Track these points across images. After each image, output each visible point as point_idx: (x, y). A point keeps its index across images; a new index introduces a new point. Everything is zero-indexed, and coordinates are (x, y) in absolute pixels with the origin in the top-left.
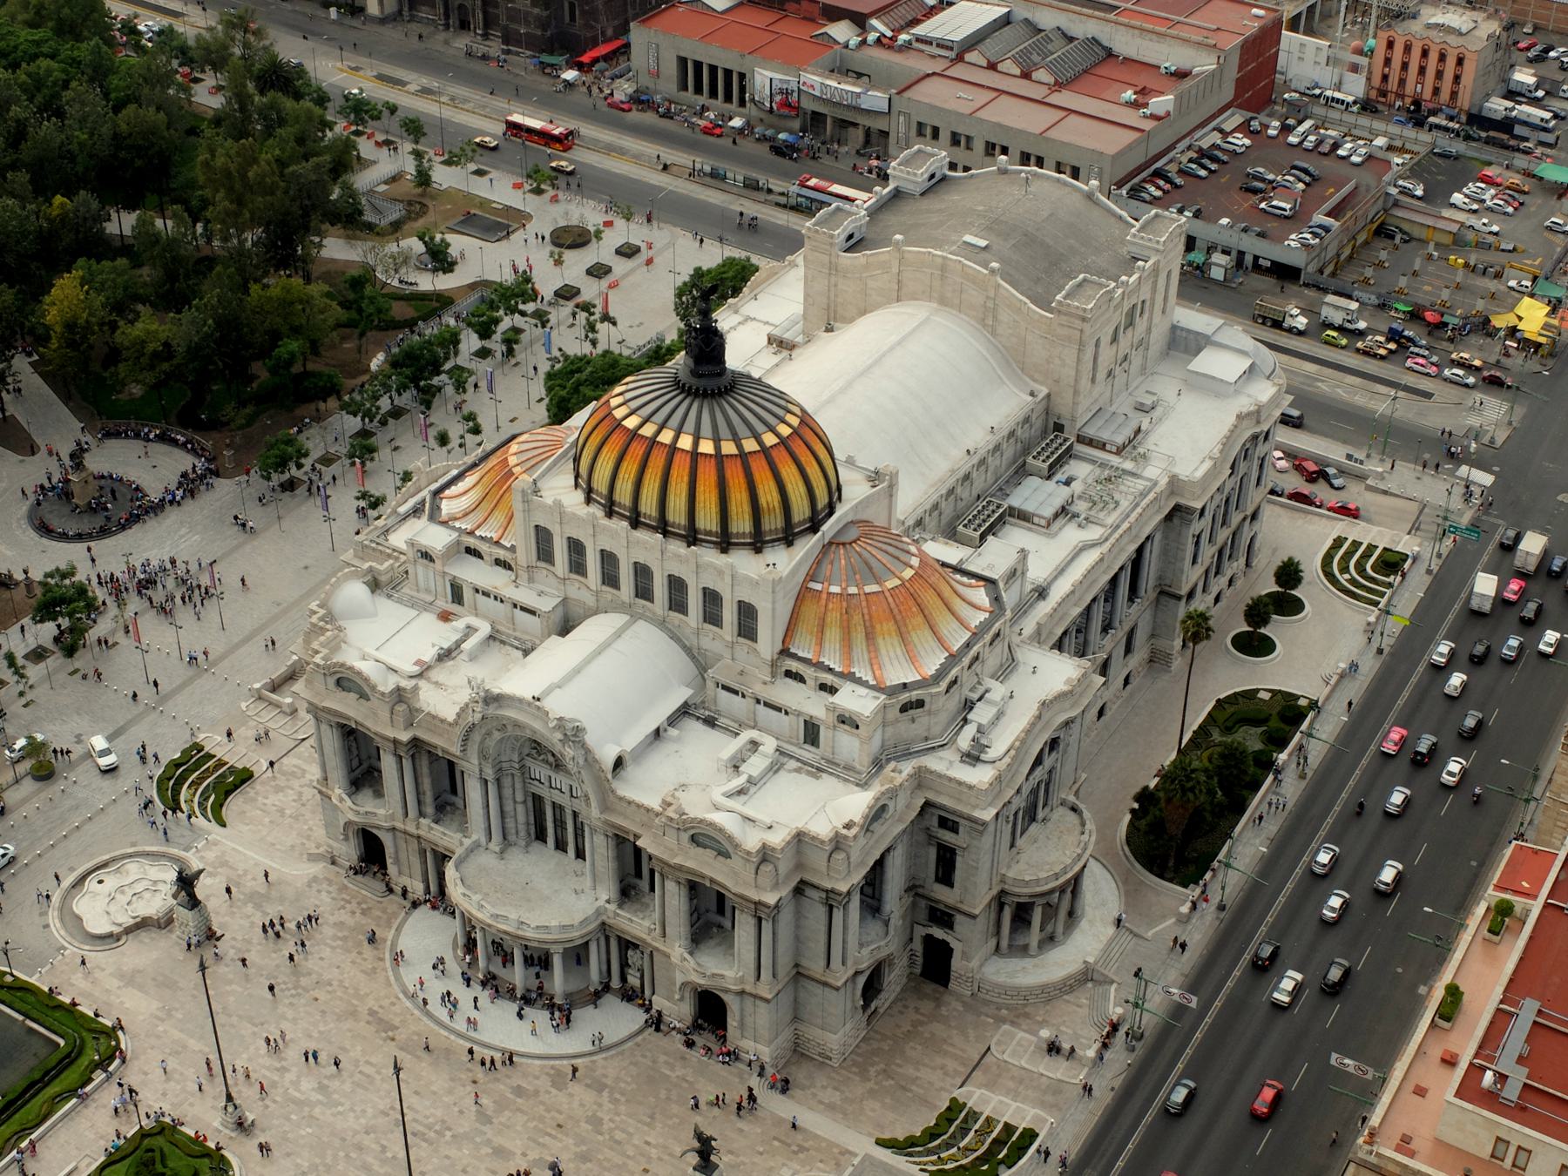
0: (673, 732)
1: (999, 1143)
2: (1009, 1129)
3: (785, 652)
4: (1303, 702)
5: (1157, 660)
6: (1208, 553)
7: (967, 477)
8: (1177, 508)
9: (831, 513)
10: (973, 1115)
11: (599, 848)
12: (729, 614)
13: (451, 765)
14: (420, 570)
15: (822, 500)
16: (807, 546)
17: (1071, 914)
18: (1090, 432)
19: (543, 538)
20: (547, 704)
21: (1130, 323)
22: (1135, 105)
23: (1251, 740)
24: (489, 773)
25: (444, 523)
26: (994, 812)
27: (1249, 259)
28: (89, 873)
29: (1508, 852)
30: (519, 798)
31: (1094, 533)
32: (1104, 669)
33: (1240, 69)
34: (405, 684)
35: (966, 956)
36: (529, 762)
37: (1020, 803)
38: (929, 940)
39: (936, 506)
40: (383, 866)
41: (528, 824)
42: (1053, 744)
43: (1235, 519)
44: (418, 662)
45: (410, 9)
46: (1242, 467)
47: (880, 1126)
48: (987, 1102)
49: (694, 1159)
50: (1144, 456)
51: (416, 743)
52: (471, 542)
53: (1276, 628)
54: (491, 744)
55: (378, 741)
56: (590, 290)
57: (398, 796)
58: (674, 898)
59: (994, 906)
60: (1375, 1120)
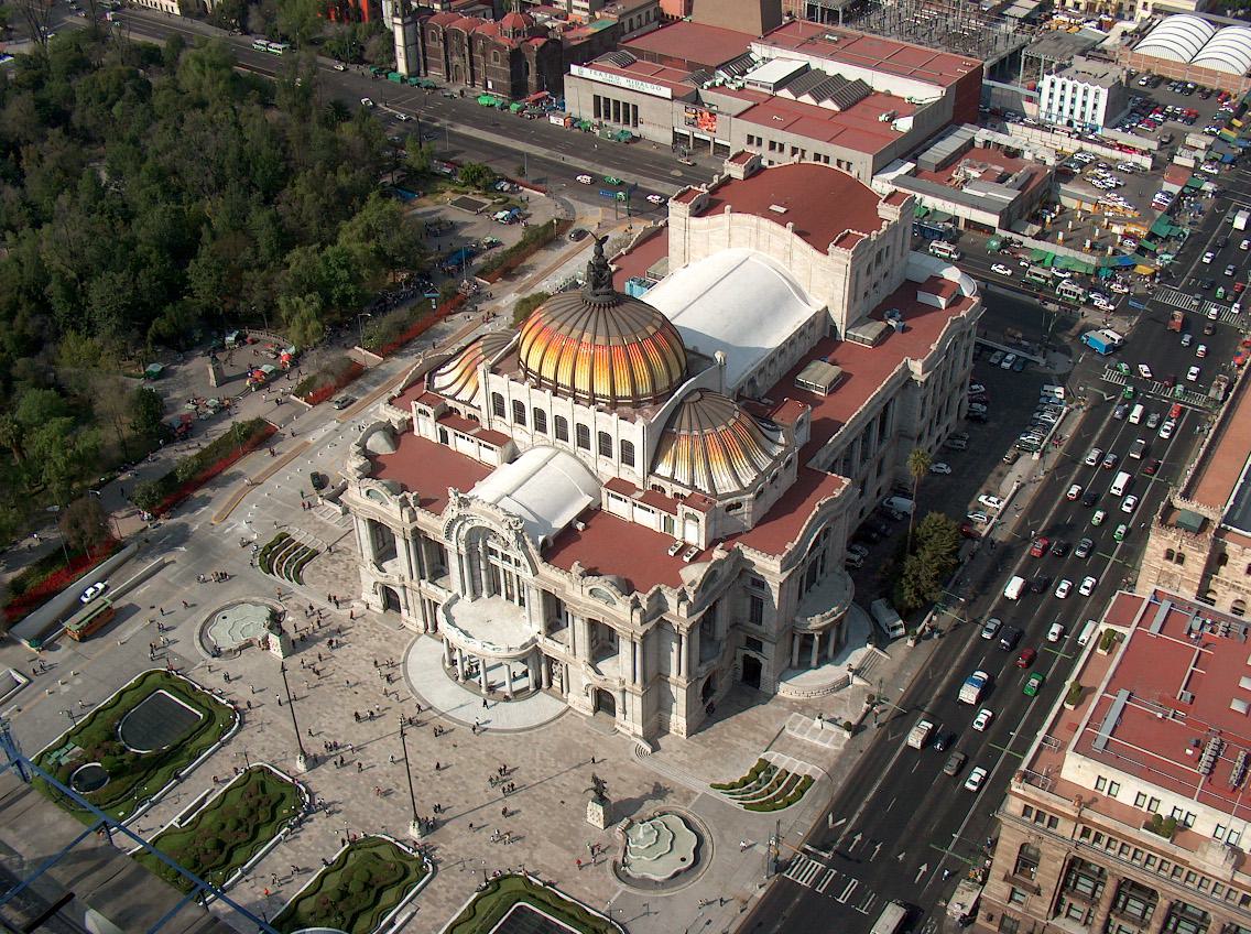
0: (580, 526)
1: (788, 789)
2: (797, 777)
7: (773, 361)
12: (616, 449)
17: (838, 642)
19: (498, 400)
21: (879, 259)
24: (463, 549)
26: (786, 574)
28: (218, 612)
29: (1114, 599)
41: (488, 583)
42: (826, 532)
45: (426, 69)
48: (783, 760)
49: (592, 794)
51: (416, 531)
54: (463, 533)
55: (394, 530)
57: (407, 566)
58: (579, 632)
59: (789, 636)
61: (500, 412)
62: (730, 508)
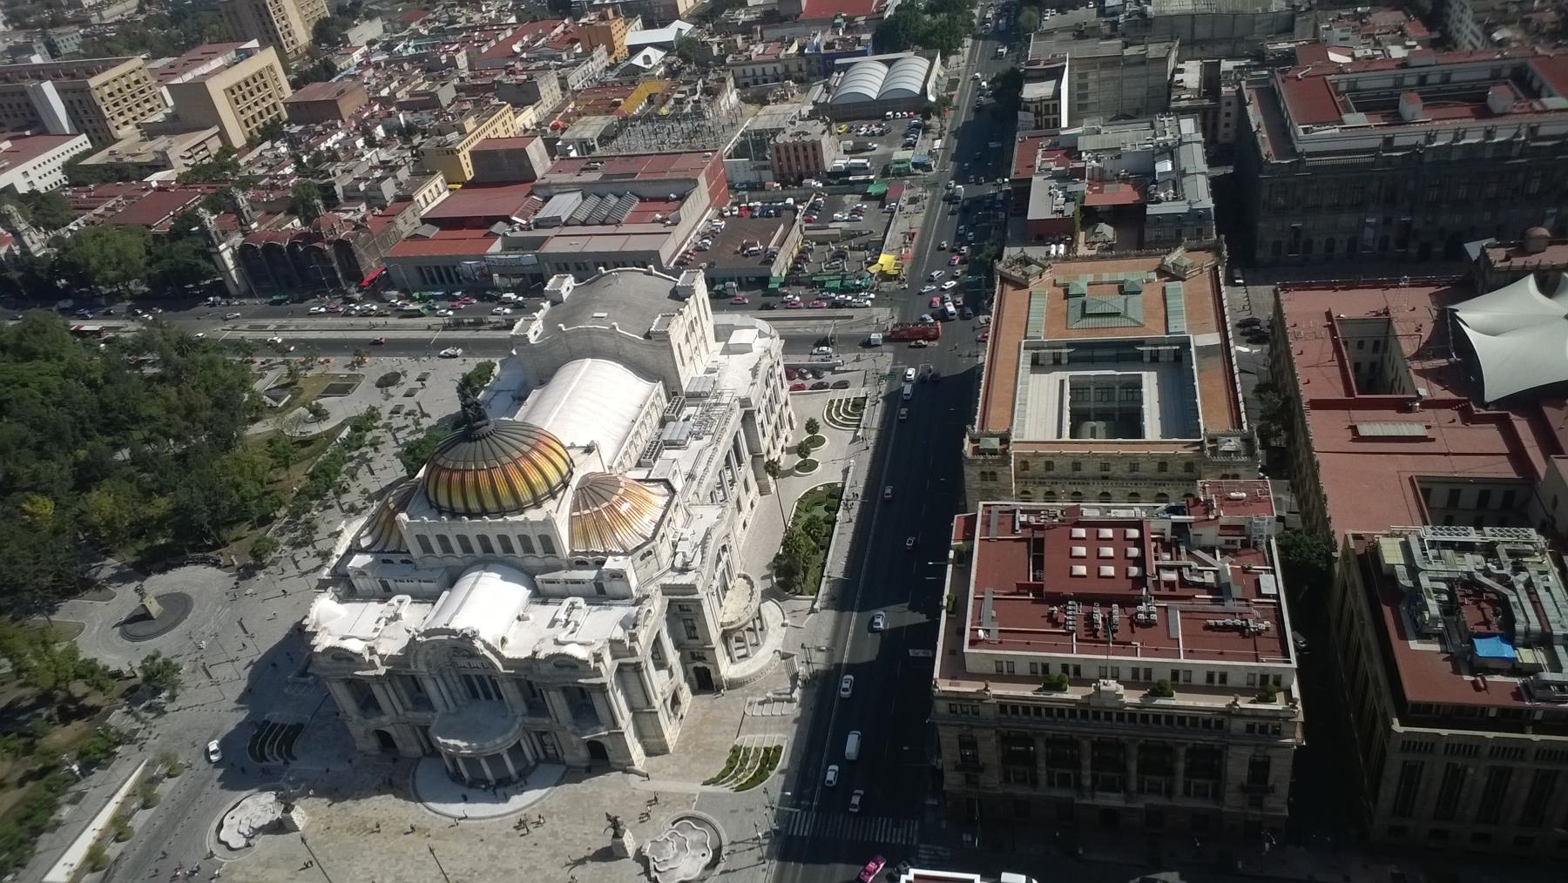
2: (767, 750)
3: (573, 553)
5: (764, 491)
6: (769, 429)
10: (747, 750)
11: (510, 692)
12: (537, 545)
13: (413, 677)
15: (565, 470)
20: (451, 627)
22: (662, 221)
23: (820, 512)
30: (456, 679)
31: (707, 439)
34: (371, 644)
35: (717, 671)
36: (456, 659)
37: (716, 584)
40: (394, 746)
43: (777, 408)
46: (772, 382)
47: (704, 775)
52: (385, 556)
56: (409, 404)
61: (427, 548)
62: (642, 558)
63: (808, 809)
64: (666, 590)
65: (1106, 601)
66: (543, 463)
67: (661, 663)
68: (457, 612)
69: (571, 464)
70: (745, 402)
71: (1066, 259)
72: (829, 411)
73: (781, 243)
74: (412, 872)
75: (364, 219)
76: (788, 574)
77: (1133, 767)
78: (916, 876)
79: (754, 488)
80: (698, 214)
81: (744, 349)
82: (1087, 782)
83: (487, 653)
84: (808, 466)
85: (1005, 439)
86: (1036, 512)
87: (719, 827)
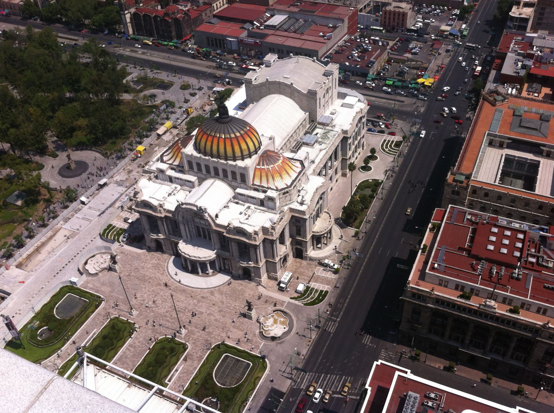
1: (319, 296)
2: (322, 291)
4: (380, 181)
5: (344, 175)
6: (353, 147)
8: (344, 137)
9: (260, 149)
10: (313, 289)
11: (214, 237)
12: (238, 177)
13: (175, 221)
14: (160, 175)
16: (255, 157)
18: (321, 121)
19: (190, 163)
22: (323, 36)
23: (368, 192)
25: (165, 163)
27: (355, 73)
31: (323, 146)
32: (331, 179)
33: (349, 23)
34: (161, 203)
37: (314, 213)
38: (296, 249)
39: (285, 144)
40: (162, 248)
42: (321, 198)
43: (359, 138)
44: (164, 198)
46: (359, 125)
47: (291, 295)
50: (334, 126)
53: (371, 164)
58: (234, 248)
60: (410, 279)
62: (284, 194)
63: (335, 321)
64: (292, 210)
65: (500, 264)
66: (248, 140)
67: (282, 242)
68: (199, 199)
69: (260, 143)
70: (345, 132)
71: (516, 97)
72: (382, 145)
73: (376, 58)
74: (161, 302)
75: (188, 10)
76: (348, 218)
77: (491, 340)
78: (381, 363)
79: (340, 173)
80: (340, 37)
81: (351, 106)
82: (467, 342)
83: (209, 219)
84: (366, 168)
85: (468, 177)
86: (476, 215)
87: (294, 318)
